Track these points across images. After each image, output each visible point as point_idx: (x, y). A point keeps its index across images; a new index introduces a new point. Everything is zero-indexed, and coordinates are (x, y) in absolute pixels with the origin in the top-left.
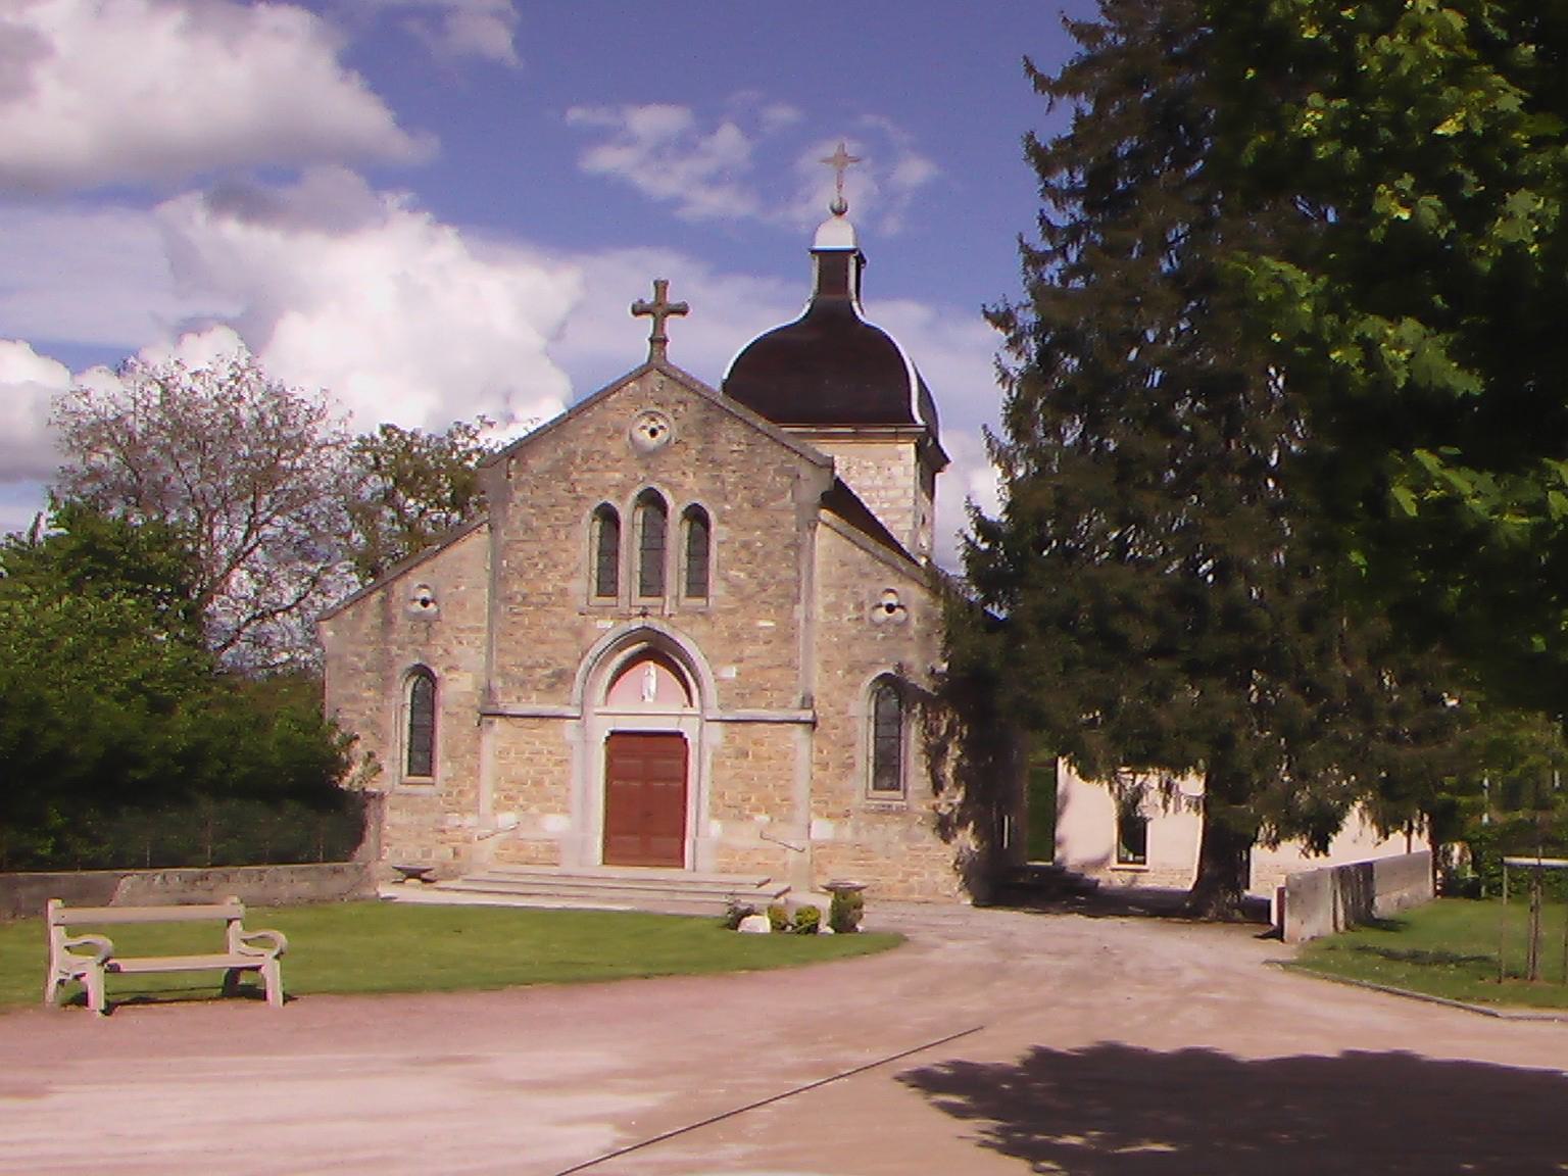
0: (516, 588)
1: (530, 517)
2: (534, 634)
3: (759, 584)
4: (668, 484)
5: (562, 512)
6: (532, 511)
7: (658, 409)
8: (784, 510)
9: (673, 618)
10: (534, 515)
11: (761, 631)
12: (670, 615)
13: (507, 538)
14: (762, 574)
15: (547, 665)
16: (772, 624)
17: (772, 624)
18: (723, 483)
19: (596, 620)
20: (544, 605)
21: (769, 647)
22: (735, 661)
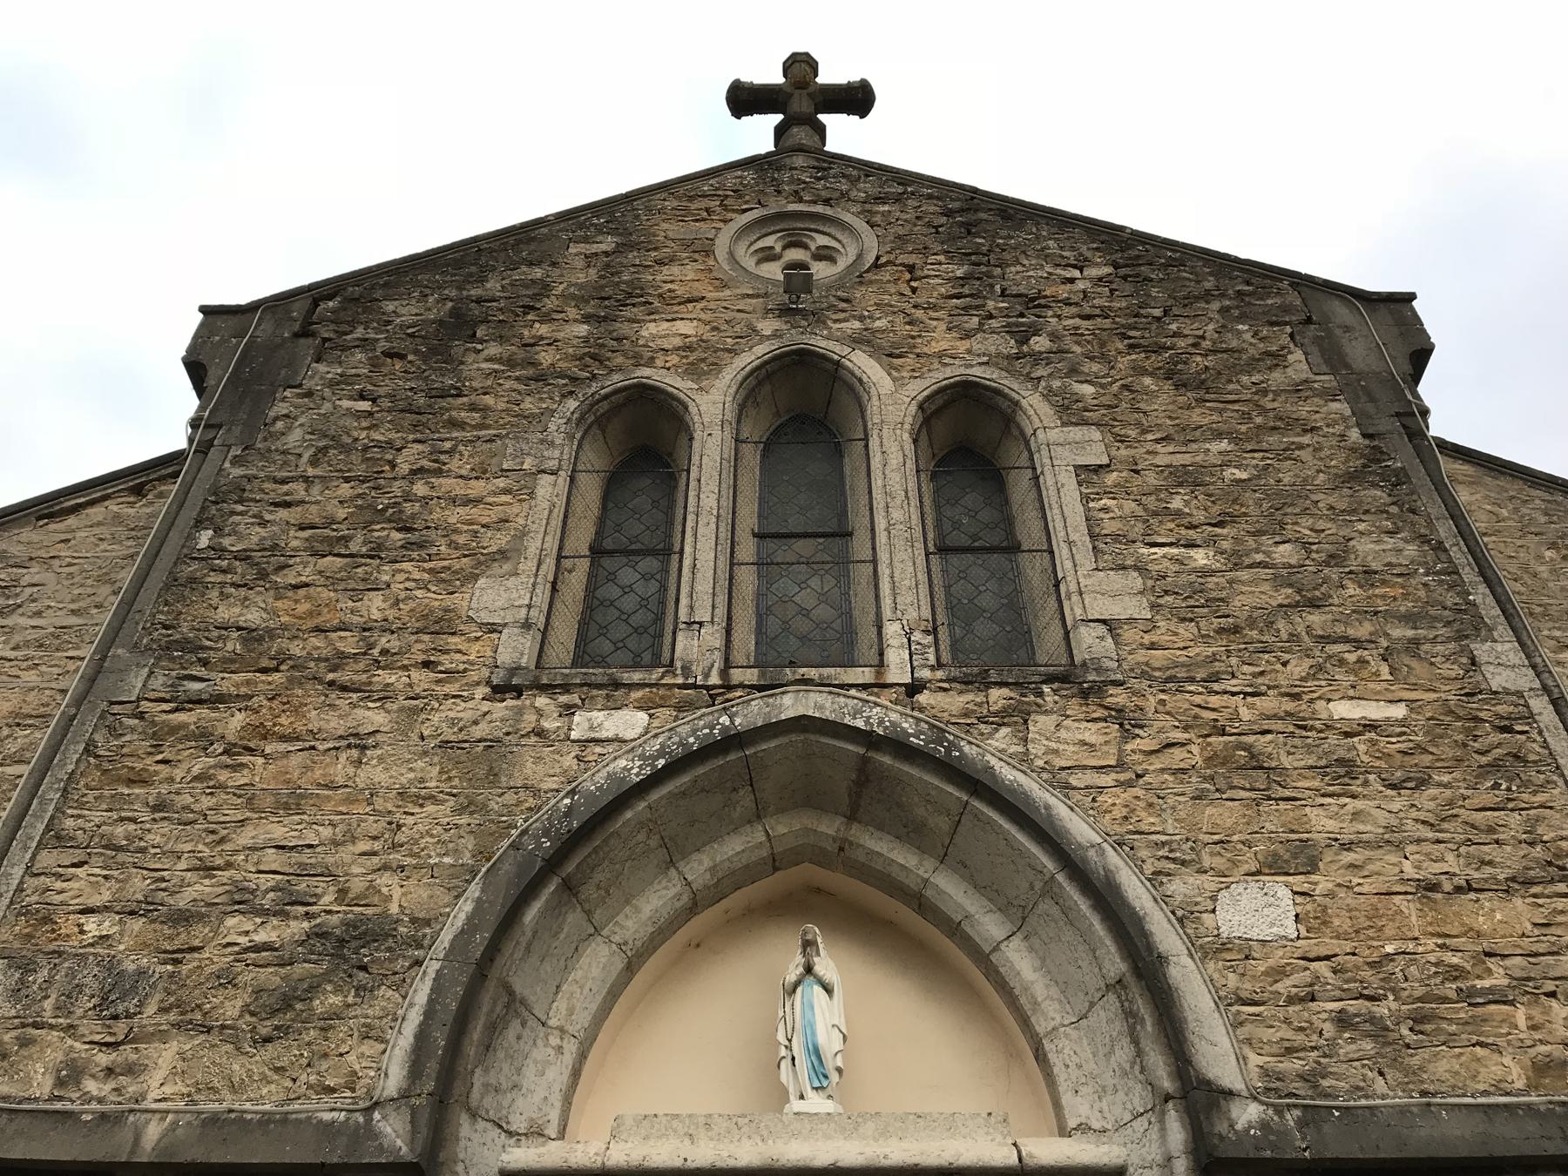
0: (225, 613)
1: (350, 422)
2: (258, 772)
3: (1279, 582)
4: (856, 341)
5: (473, 408)
6: (365, 405)
7: (819, 209)
8: (1298, 390)
9: (923, 698)
10: (370, 414)
11: (1360, 745)
12: (914, 688)
13: (237, 472)
14: (1285, 553)
15: (289, 902)
16: (1399, 711)
17: (1399, 711)
18: (1054, 337)
19: (568, 710)
20: (339, 660)
21: (1427, 799)
22: (1274, 866)
